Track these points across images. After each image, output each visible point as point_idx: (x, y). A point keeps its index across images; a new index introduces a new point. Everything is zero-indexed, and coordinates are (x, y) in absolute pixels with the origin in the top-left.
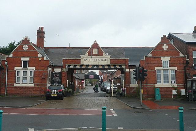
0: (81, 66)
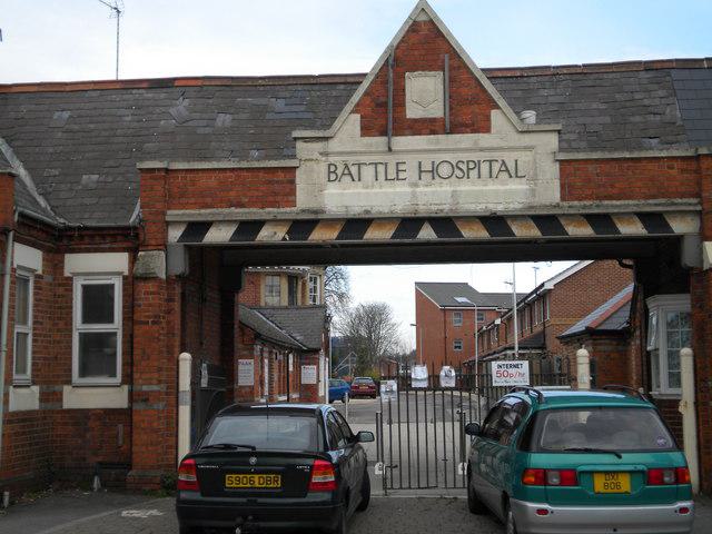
0: (302, 226)
